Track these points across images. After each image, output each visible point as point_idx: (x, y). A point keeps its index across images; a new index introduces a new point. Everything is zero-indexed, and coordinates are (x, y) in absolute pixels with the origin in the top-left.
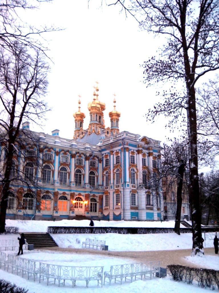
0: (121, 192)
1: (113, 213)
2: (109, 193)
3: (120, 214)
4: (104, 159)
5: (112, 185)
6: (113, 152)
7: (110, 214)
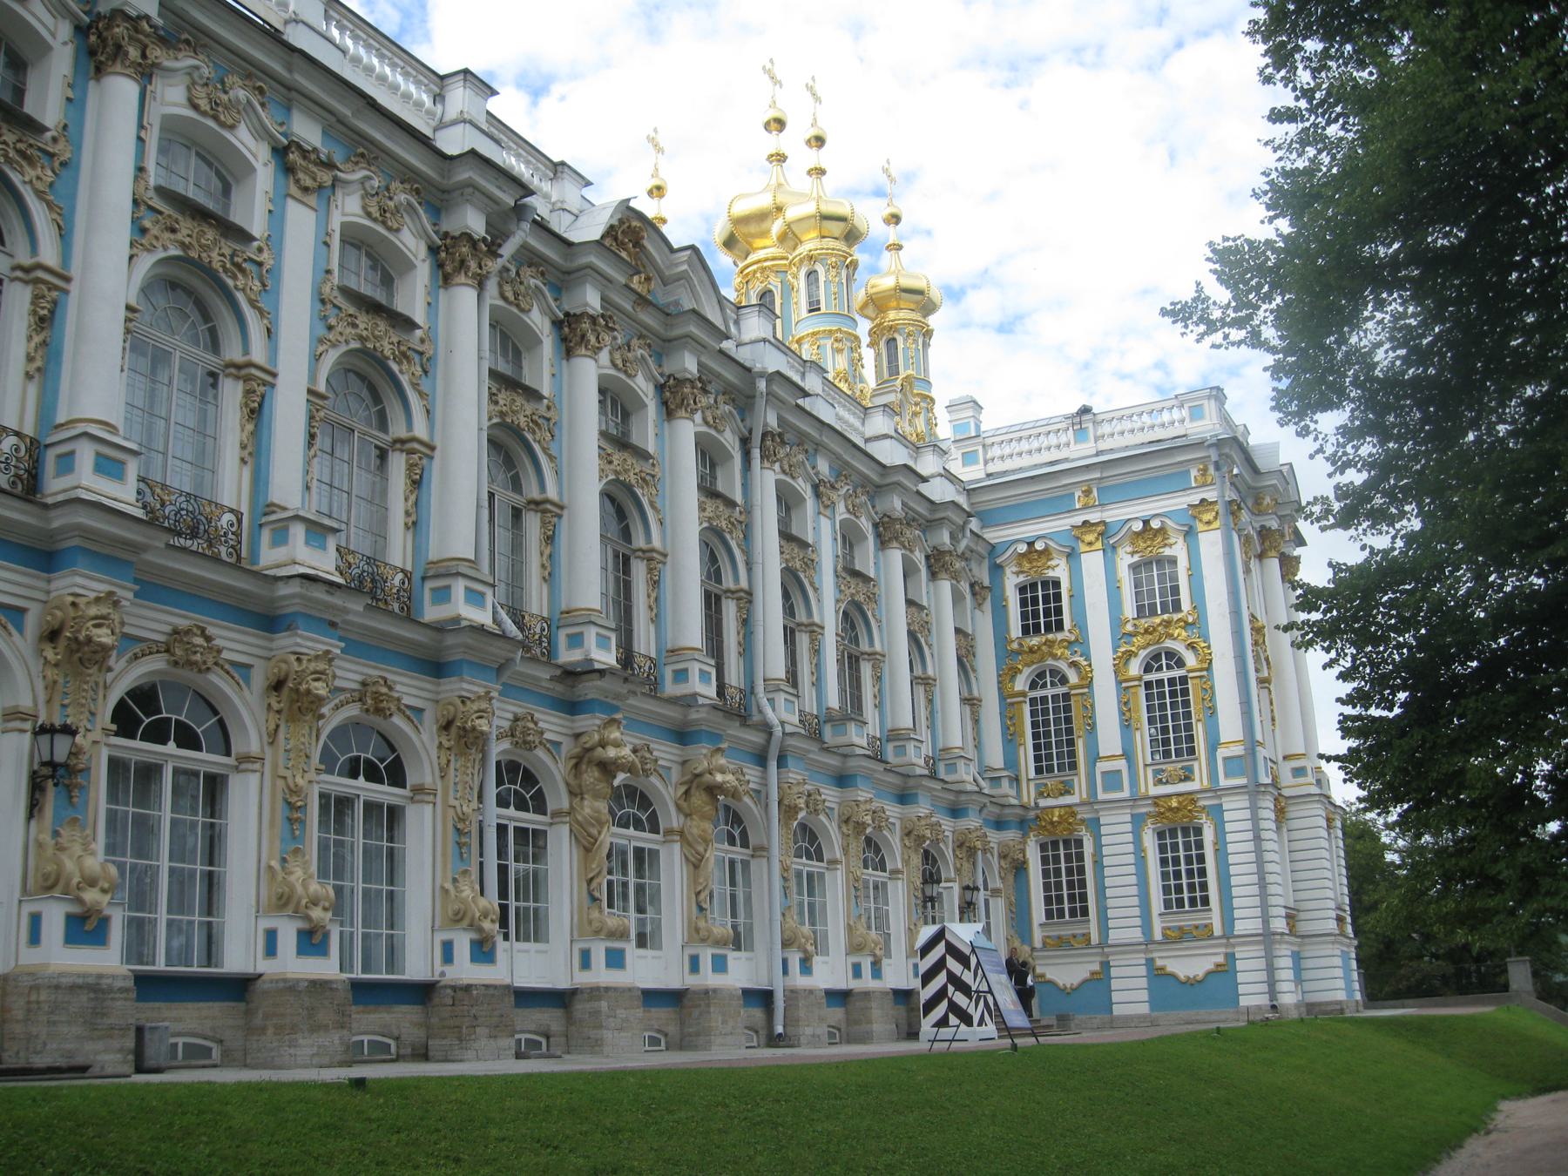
0: (1217, 813)
1: (1150, 962)
2: (1095, 825)
3: (1226, 971)
4: (1011, 582)
5: (1121, 764)
6: (1104, 531)
7: (1113, 972)
